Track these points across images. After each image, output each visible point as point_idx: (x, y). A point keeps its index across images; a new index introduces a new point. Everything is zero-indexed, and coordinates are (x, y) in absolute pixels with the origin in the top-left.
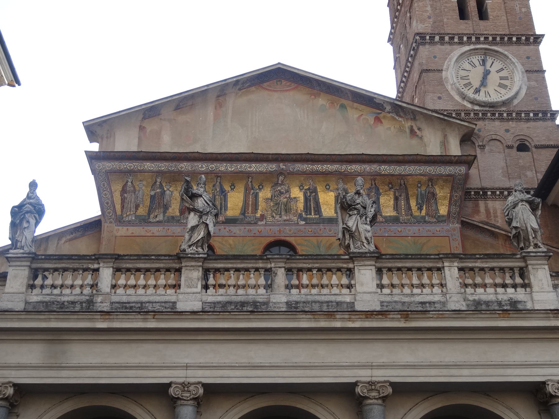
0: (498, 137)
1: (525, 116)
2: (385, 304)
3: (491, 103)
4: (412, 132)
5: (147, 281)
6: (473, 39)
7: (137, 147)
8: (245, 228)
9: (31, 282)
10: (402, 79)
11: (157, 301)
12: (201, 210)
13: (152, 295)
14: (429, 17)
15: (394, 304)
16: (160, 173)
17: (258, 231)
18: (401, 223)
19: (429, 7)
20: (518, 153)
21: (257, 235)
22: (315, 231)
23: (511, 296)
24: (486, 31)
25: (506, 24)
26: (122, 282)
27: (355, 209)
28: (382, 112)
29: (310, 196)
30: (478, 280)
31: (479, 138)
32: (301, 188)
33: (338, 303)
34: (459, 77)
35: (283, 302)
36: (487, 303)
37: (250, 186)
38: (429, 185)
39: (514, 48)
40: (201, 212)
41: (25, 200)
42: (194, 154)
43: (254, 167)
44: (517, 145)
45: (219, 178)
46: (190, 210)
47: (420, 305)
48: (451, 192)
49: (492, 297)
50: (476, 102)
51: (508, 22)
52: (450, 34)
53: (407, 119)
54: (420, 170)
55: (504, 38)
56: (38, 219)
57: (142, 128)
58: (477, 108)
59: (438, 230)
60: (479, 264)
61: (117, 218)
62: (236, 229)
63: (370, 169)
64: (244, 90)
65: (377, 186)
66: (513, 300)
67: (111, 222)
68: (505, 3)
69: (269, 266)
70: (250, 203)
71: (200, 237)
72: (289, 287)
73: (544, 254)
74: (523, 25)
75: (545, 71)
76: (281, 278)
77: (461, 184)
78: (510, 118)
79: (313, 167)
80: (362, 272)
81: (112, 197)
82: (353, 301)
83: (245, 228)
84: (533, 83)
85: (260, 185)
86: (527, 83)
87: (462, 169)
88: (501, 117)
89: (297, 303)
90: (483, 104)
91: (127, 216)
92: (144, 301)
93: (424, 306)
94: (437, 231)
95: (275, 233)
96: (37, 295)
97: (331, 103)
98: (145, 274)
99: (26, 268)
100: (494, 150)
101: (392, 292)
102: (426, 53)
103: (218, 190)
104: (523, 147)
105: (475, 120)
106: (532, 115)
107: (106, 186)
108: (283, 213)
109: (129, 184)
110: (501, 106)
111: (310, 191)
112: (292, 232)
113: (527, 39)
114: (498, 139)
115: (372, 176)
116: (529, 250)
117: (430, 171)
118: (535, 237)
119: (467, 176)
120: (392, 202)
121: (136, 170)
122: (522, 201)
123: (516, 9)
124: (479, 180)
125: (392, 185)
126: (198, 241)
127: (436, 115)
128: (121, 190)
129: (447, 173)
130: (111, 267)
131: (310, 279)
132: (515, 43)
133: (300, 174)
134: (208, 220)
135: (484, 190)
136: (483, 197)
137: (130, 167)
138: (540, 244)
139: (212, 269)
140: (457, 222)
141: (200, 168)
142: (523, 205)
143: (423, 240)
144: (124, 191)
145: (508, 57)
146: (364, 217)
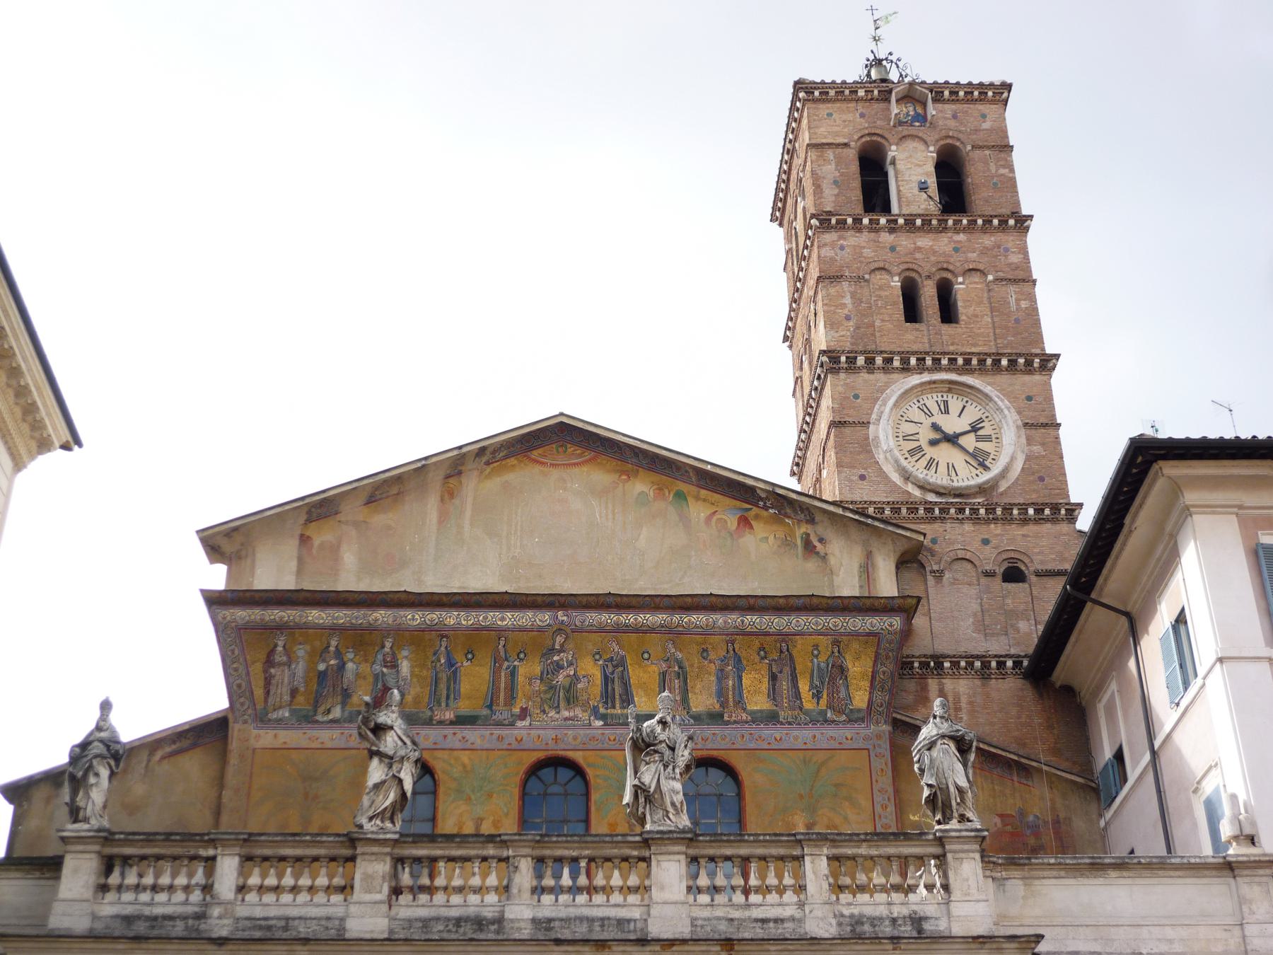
0: (969, 553)
1: (1019, 514)
2: (700, 922)
3: (957, 488)
4: (808, 547)
5: (297, 880)
6: (929, 362)
7: (294, 577)
8: (492, 734)
9: (102, 881)
10: (802, 427)
11: (313, 916)
12: (391, 753)
13: (305, 905)
14: (848, 318)
15: (715, 922)
16: (334, 629)
17: (517, 740)
18: (782, 723)
19: (848, 297)
20: (1006, 585)
21: (513, 747)
22: (621, 739)
23: (915, 908)
24: (952, 344)
25: (991, 331)
26: (254, 880)
27: (656, 752)
28: (750, 507)
29: (613, 673)
30: (862, 878)
31: (933, 556)
32: (597, 657)
33: (621, 923)
34: (901, 435)
35: (527, 919)
36: (874, 921)
37: (502, 654)
39: (1004, 379)
40: (391, 758)
41: (91, 734)
42: (398, 596)
43: (509, 618)
44: (1002, 570)
46: (372, 754)
47: (760, 924)
48: (874, 665)
49: (882, 911)
50: (928, 487)
51: (994, 328)
52: (886, 352)
53: (799, 521)
54: (817, 623)
55: (985, 360)
56: (114, 768)
57: (304, 540)
58: (931, 497)
59: (849, 738)
60: (863, 850)
62: (474, 735)
63: (725, 622)
64: (495, 465)
66: (917, 916)
67: (245, 722)
68: (989, 290)
69: (505, 853)
70: (503, 685)
71: (388, 803)
72: (538, 890)
73: (973, 834)
74: (1021, 334)
75: (1059, 425)
76: (524, 876)
77: (892, 650)
78: (991, 516)
79: (619, 618)
80: (665, 865)
81: (248, 674)
82: (645, 917)
83: (492, 734)
84: (1037, 449)
86: (1026, 449)
87: (895, 622)
88: (974, 516)
89: (550, 920)
90: (942, 491)
91: (275, 710)
92: (291, 916)
93: (765, 926)
94: (847, 739)
95: (547, 744)
96: (111, 903)
97: (657, 489)
98: (293, 867)
99: (93, 856)
100: (960, 578)
101: (712, 900)
102: (840, 389)
103: (443, 661)
104: (1013, 575)
105: (927, 521)
106: (1031, 511)
107: (236, 652)
108: (562, 704)
109: (280, 649)
110: (974, 495)
111: (614, 663)
112: (579, 740)
113: (1029, 363)
114: (967, 557)
115: (727, 635)
116: (947, 827)
117: (835, 626)
118: (963, 800)
119: (907, 633)
120: (765, 686)
121: (291, 624)
122: (943, 736)
123: (1009, 303)
124: (930, 639)
125: (765, 652)
126: (386, 809)
127: (851, 515)
128: (264, 660)
129: (868, 631)
130: (236, 854)
131: (574, 876)
132: (1007, 370)
134: (403, 771)
135: (938, 659)
136: (935, 672)
137: (282, 618)
138: (970, 815)
139: (408, 858)
140: (885, 722)
141: (410, 620)
142: (944, 744)
143: (821, 756)
144: (269, 662)
145: (990, 399)
146: (671, 767)
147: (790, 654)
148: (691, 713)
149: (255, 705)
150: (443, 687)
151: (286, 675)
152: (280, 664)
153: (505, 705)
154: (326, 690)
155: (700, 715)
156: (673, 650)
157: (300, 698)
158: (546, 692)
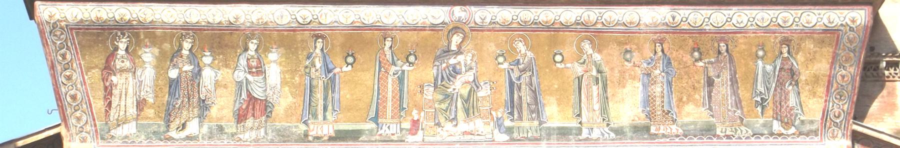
29: (519, 79)
32: (501, 59)
37: (389, 57)
38: (781, 53)
45: (320, 40)
48: (831, 69)
61: (96, 131)
65: (666, 55)
70: (390, 95)
85: (410, 54)
91: (119, 125)
107: (68, 57)
109: (121, 52)
115: (656, 33)
117: (785, 22)
121: (135, 23)
125: (701, 54)
128: (102, 66)
129: (824, 28)
133: (498, 31)
140: (843, 135)
147: (730, 56)
148: (612, 125)
149: (94, 120)
150: (319, 95)
151: (131, 83)
152: (122, 71)
153: (393, 117)
154: (179, 102)
155: (622, 128)
156: (590, 51)
157: (150, 112)
158: (441, 102)
